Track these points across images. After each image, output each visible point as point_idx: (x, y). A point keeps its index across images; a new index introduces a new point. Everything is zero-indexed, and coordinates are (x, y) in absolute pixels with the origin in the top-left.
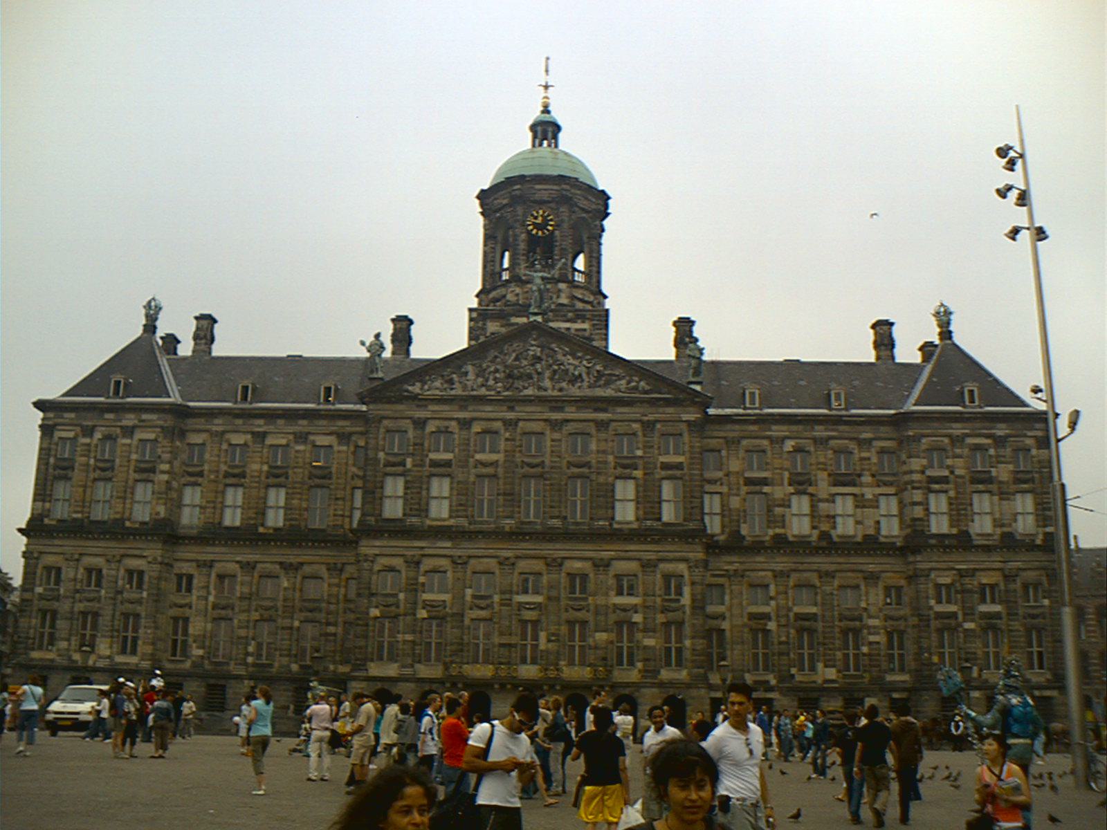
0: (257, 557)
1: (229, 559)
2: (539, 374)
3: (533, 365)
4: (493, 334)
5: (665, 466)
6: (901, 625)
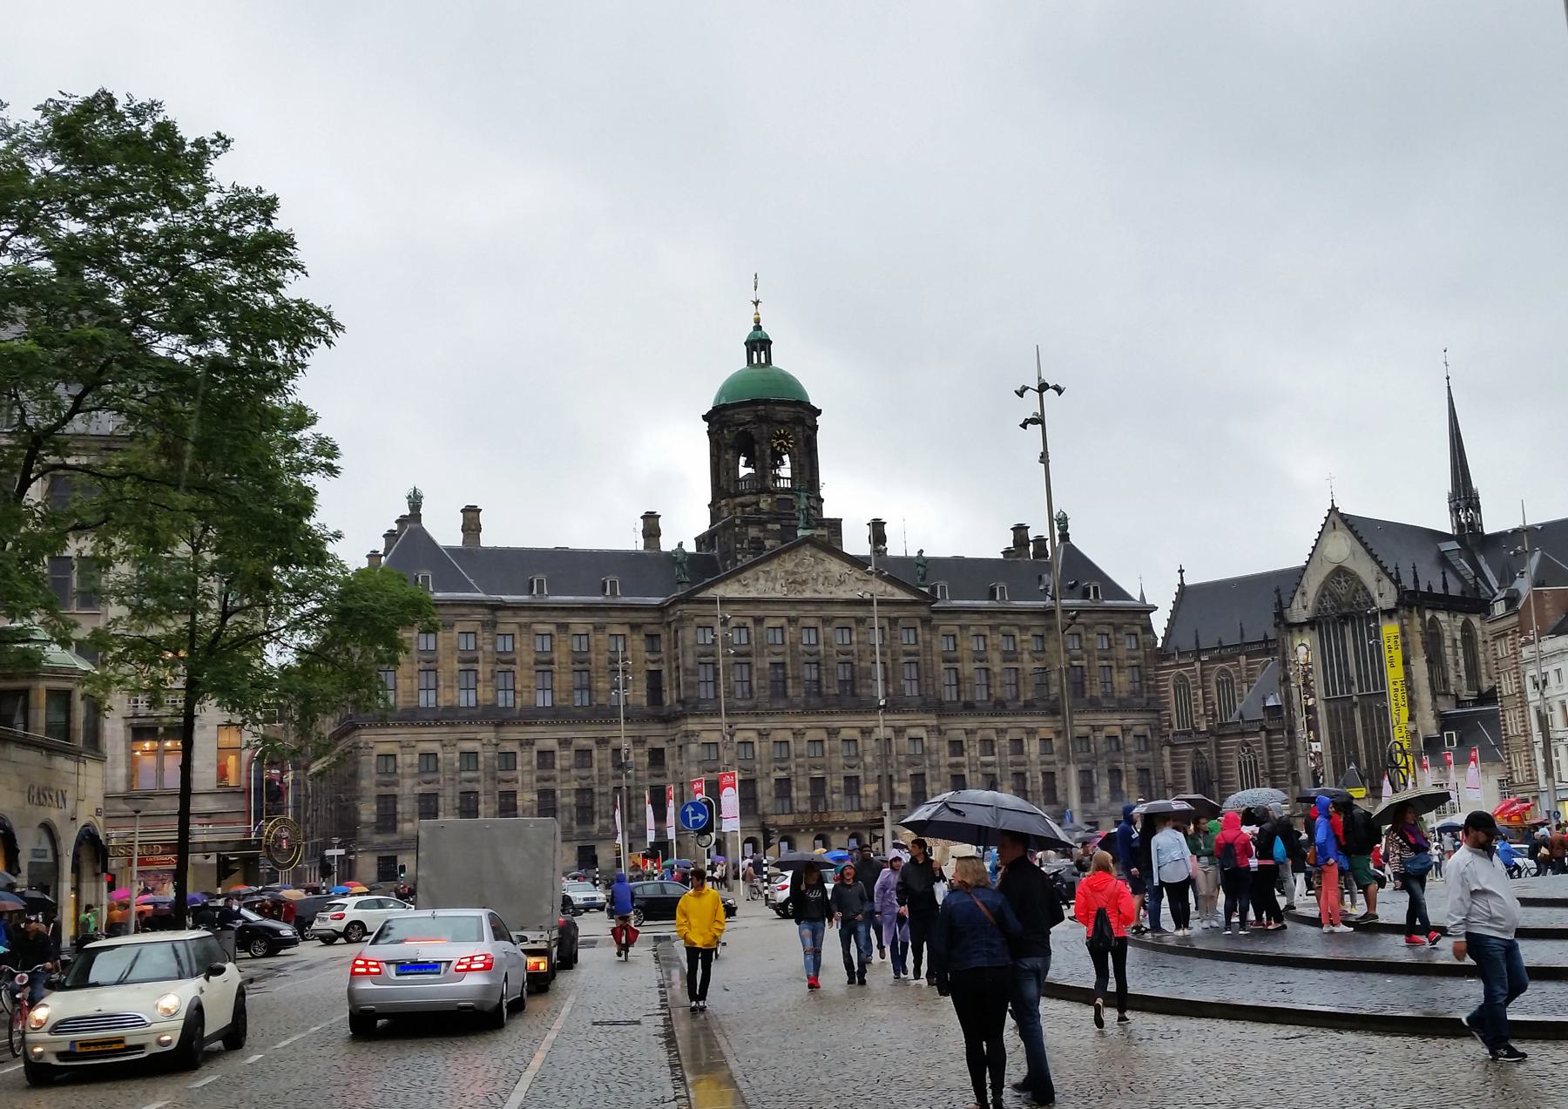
0: (572, 734)
1: (547, 738)
5: (907, 654)
6: (1051, 768)
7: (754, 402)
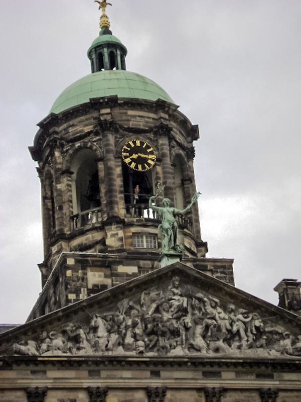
2: (187, 329)
3: (178, 319)
4: (95, 286)
7: (95, 104)
